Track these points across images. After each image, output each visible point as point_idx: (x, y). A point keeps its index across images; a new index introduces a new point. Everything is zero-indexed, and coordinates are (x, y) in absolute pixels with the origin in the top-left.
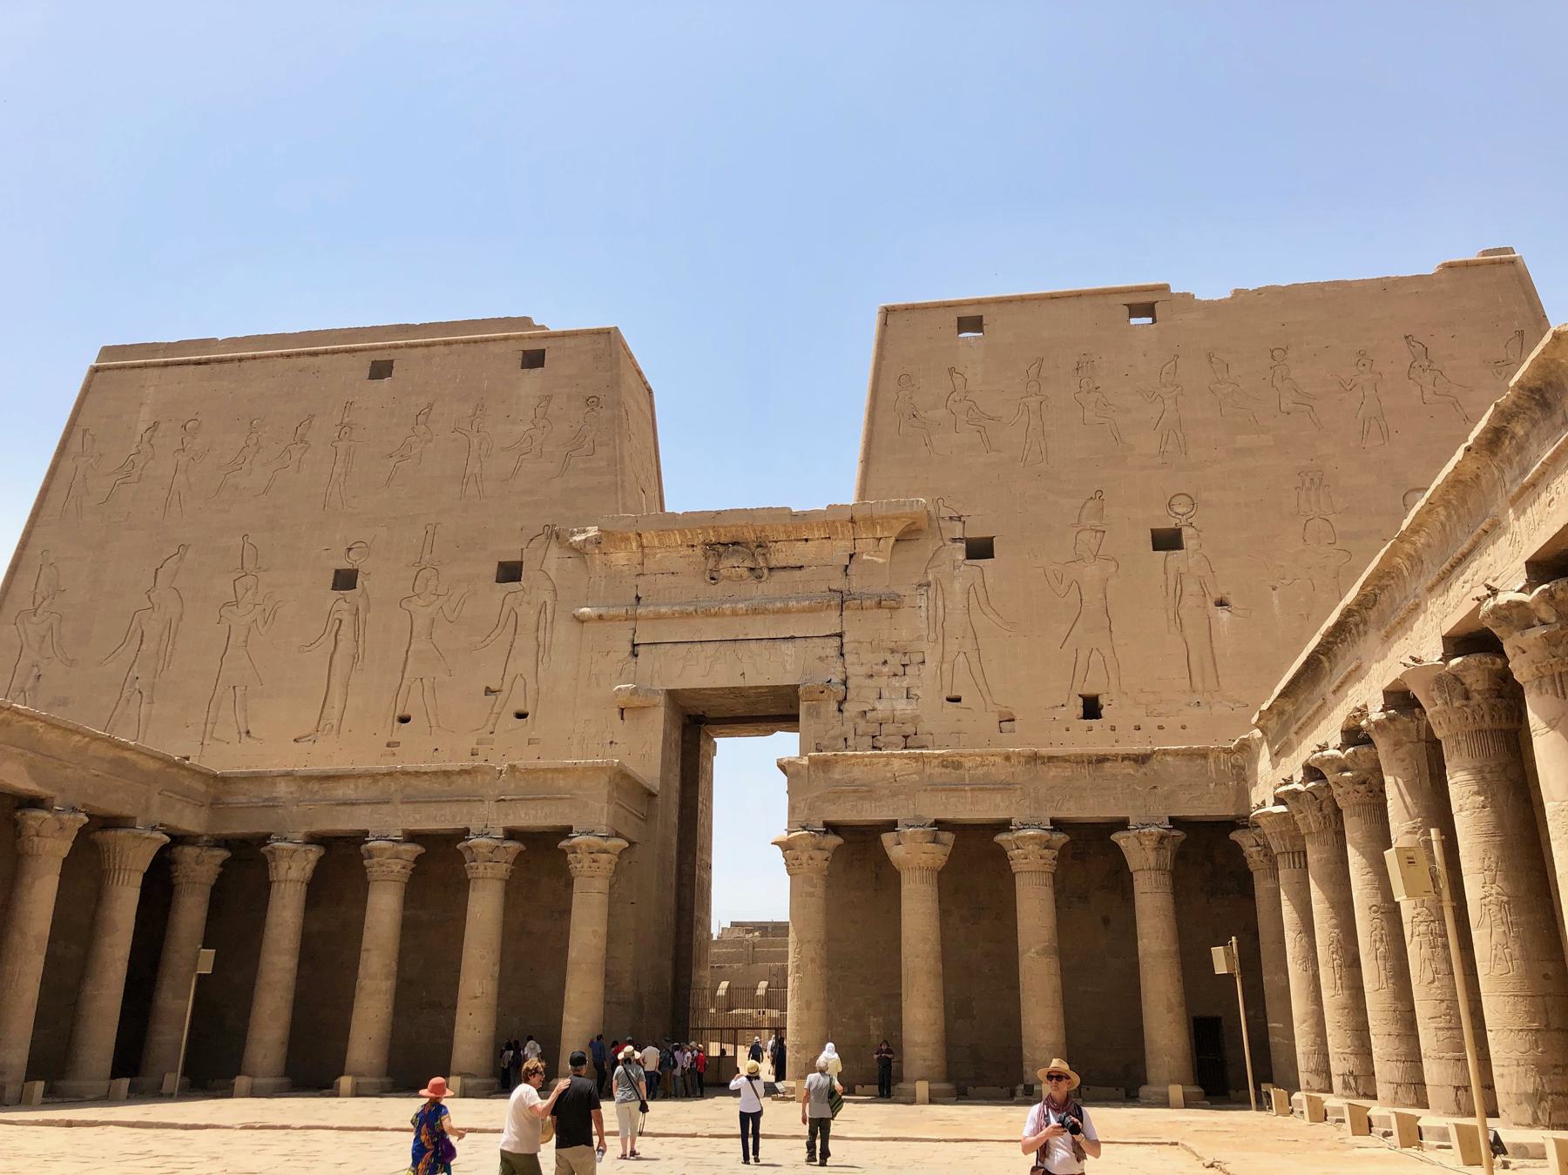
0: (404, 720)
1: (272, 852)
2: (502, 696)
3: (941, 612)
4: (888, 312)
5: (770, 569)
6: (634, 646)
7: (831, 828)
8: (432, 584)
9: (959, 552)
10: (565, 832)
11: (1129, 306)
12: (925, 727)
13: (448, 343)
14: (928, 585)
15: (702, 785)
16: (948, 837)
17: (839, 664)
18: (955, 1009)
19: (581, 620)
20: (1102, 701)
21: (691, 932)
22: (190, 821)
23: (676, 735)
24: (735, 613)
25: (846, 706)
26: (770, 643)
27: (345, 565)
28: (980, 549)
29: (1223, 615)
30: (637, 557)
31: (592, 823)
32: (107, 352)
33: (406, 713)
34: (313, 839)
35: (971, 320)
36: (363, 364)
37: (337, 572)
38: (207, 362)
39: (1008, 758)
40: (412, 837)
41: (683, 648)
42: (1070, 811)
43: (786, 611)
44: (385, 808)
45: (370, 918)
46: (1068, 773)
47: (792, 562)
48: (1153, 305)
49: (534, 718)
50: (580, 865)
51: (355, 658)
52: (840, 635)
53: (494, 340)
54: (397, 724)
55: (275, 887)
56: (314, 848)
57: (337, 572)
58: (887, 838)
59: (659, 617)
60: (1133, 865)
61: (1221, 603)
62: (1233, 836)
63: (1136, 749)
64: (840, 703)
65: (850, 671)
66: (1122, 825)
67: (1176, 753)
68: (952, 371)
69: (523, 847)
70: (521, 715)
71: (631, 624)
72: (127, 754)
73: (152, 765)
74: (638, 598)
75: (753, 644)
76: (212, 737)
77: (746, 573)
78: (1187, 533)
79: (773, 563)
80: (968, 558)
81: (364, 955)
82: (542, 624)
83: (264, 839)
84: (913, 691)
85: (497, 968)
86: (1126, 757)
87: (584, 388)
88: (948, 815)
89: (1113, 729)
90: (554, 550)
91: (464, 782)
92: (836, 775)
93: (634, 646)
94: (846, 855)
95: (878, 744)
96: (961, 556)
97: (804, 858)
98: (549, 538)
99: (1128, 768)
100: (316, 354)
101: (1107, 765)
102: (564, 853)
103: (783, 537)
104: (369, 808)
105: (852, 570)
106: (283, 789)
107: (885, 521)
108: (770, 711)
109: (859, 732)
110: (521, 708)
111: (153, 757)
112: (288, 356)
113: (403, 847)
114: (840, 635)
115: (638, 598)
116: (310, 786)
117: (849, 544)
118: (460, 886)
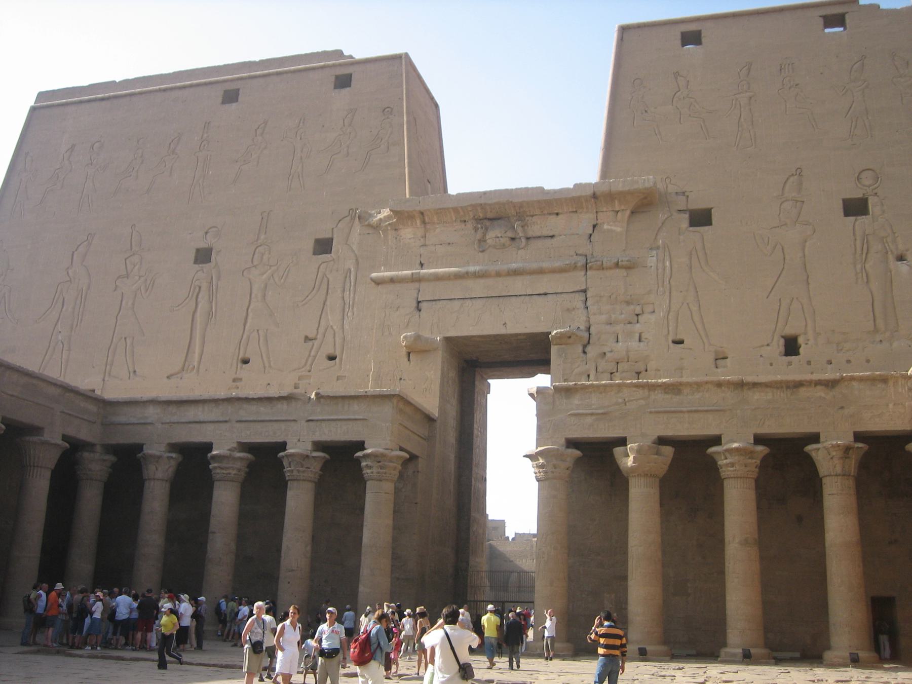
0: (246, 362)
2: (316, 343)
3: (668, 271)
5: (528, 239)
6: (419, 302)
7: (572, 443)
8: (266, 257)
9: (685, 219)
10: (361, 446)
11: (825, 18)
12: (652, 365)
13: (278, 74)
14: (658, 248)
15: (477, 416)
16: (669, 451)
17: (585, 311)
18: (673, 587)
19: (378, 282)
20: (801, 340)
21: (468, 529)
22: (84, 434)
23: (453, 374)
24: (498, 274)
25: (588, 349)
26: (527, 298)
27: (202, 245)
28: (701, 218)
29: (903, 267)
30: (420, 232)
31: (380, 439)
32: (42, 96)
33: (247, 356)
36: (217, 94)
37: (198, 250)
38: (108, 98)
39: (719, 385)
41: (457, 304)
42: (772, 428)
43: (541, 272)
44: (224, 426)
45: (215, 510)
46: (769, 396)
47: (546, 232)
49: (341, 360)
50: (369, 470)
51: (209, 314)
52: (585, 291)
53: (314, 69)
54: (240, 364)
55: (147, 484)
56: (174, 455)
57: (198, 250)
58: (618, 451)
60: (822, 471)
61: (901, 258)
63: (828, 376)
64: (585, 346)
65: (593, 319)
66: (815, 438)
67: (861, 379)
69: (327, 456)
70: (332, 358)
71: (417, 285)
72: (35, 381)
73: (52, 391)
76: (110, 374)
77: (508, 242)
79: (530, 234)
81: (211, 536)
83: (139, 447)
84: (643, 336)
85: (309, 548)
86: (819, 383)
87: (382, 103)
88: (669, 433)
89: (809, 363)
90: (357, 228)
91: (283, 406)
92: (576, 400)
94: (584, 466)
96: (685, 224)
98: (353, 219)
99: (820, 392)
100: (184, 87)
102: (358, 461)
104: (211, 427)
106: (152, 413)
107: (621, 196)
108: (526, 355)
109: (599, 369)
110: (330, 351)
111: (55, 385)
112: (165, 90)
114: (585, 291)
115: (422, 265)
117: (592, 216)
118: (280, 486)
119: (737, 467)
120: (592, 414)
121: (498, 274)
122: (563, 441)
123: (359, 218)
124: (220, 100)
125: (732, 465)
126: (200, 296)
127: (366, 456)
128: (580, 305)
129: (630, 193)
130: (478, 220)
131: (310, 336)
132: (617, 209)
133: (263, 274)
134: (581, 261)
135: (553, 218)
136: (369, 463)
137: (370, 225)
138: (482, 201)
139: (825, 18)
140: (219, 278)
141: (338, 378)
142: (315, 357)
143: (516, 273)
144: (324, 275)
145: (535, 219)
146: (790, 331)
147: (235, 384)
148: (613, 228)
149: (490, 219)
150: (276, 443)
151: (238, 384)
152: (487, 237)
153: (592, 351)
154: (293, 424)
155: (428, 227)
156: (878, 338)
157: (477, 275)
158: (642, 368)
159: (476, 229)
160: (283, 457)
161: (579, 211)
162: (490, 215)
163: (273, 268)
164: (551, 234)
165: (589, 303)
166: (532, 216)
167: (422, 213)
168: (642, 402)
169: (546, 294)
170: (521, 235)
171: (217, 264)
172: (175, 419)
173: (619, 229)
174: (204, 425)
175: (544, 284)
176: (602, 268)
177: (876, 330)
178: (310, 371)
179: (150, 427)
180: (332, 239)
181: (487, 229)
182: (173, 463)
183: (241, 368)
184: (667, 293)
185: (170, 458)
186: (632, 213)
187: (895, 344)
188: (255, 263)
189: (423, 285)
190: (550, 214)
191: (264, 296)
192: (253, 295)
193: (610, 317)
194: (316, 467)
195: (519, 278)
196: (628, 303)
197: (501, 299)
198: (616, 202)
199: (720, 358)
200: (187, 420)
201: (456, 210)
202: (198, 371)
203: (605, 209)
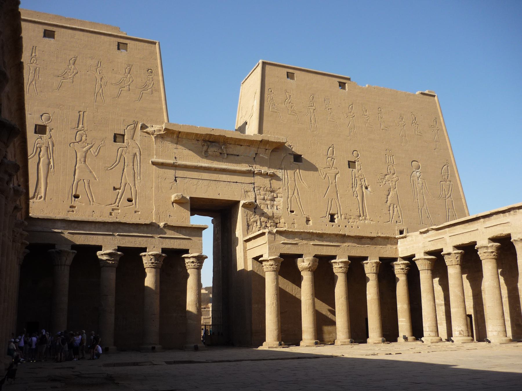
0: (76, 197)
1: (60, 252)
2: (120, 191)
6: (176, 177)
7: (282, 255)
19: (154, 163)
20: (336, 217)
25: (257, 210)
27: (40, 123)
36: (42, 28)
37: (36, 125)
41: (195, 181)
48: (345, 83)
54: (73, 198)
61: (366, 188)
68: (286, 91)
70: (130, 200)
74: (176, 158)
79: (228, 152)
80: (295, 161)
83: (53, 246)
93: (176, 177)
96: (292, 160)
101: (363, 239)
103: (233, 143)
110: (130, 197)
113: (119, 253)
115: (176, 158)
117: (256, 149)
122: (279, 255)
123: (141, 127)
124: (42, 34)
126: (41, 154)
129: (276, 143)
130: (205, 141)
131: (116, 187)
133: (83, 148)
135: (239, 147)
137: (147, 133)
138: (212, 133)
139: (339, 82)
140: (53, 146)
141: (135, 212)
142: (121, 198)
145: (231, 146)
147: (71, 209)
149: (210, 142)
152: (209, 150)
155: (179, 139)
156: (361, 218)
160: (145, 255)
162: (211, 140)
163: (89, 145)
167: (180, 132)
170: (225, 152)
171: (51, 137)
173: (266, 157)
178: (118, 206)
180: (124, 135)
181: (208, 146)
182: (74, 255)
183: (75, 200)
184: (287, 190)
185: (73, 253)
187: (366, 222)
188: (77, 141)
191: (85, 161)
192: (78, 159)
196: (272, 191)
197: (217, 182)
199: (308, 220)
201: (197, 134)
202: (45, 199)
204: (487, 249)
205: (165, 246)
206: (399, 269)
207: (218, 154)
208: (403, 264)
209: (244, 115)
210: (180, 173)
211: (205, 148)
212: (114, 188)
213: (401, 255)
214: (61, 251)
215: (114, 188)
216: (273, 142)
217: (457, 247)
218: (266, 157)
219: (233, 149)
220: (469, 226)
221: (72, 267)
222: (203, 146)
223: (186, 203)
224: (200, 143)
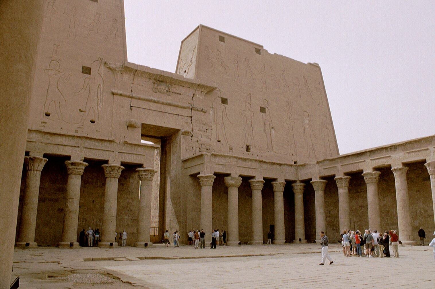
0: (48, 115)
4: (203, 27)
6: (131, 106)
11: (256, 48)
19: (113, 94)
20: (250, 147)
24: (163, 103)
25: (193, 138)
28: (224, 101)
29: (273, 131)
34: (45, 155)
35: (222, 37)
39: (256, 161)
40: (85, 160)
41: (147, 111)
44: (77, 149)
48: (260, 50)
52: (191, 117)
59: (139, 99)
60: (275, 189)
62: (293, 184)
65: (194, 128)
66: (275, 180)
68: (218, 50)
70: (93, 122)
71: (130, 99)
75: (167, 114)
78: (266, 109)
79: (173, 91)
82: (99, 92)
86: (278, 164)
90: (103, 68)
91: (108, 144)
93: (131, 106)
95: (200, 150)
96: (221, 102)
97: (210, 182)
99: (278, 167)
102: (138, 171)
104: (71, 148)
105: (194, 98)
110: (93, 119)
114: (191, 117)
116: (46, 136)
119: (260, 186)
120: (222, 165)
121: (163, 103)
123: (105, 63)
125: (259, 186)
127: (145, 171)
128: (190, 121)
129: (210, 87)
131: (82, 110)
132: (202, 91)
134: (191, 107)
136: (147, 174)
137: (109, 68)
143: (169, 105)
144: (88, 84)
145: (175, 86)
146: (248, 144)
148: (200, 97)
150: (98, 159)
151: (44, 124)
153: (195, 139)
154: (112, 153)
155: (136, 76)
157: (155, 102)
158: (208, 148)
159: (154, 83)
161: (190, 88)
162: (160, 80)
164: (180, 93)
165: (192, 122)
166: (175, 85)
168: (236, 163)
169: (178, 115)
172: (49, 141)
173: (202, 98)
174: (67, 147)
175: (178, 111)
176: (197, 110)
177: (268, 148)
178: (82, 126)
179: (33, 144)
186: (206, 93)
189: (133, 99)
190: (181, 86)
193: (199, 128)
194: (120, 171)
195: (170, 107)
198: (203, 89)
200: (55, 143)
201: (150, 74)
203: (199, 90)
204: (372, 176)
205: (124, 160)
206: (298, 188)
207: (165, 91)
208: (301, 185)
209: (183, 65)
210: (134, 103)
211: (156, 85)
212: (80, 110)
213: (300, 179)
214: (35, 158)
215: (80, 110)
216: (207, 87)
217: (346, 174)
218: (202, 98)
219: (176, 89)
220: (357, 159)
221: (44, 173)
222: (154, 83)
223: (138, 127)
224: (152, 81)
